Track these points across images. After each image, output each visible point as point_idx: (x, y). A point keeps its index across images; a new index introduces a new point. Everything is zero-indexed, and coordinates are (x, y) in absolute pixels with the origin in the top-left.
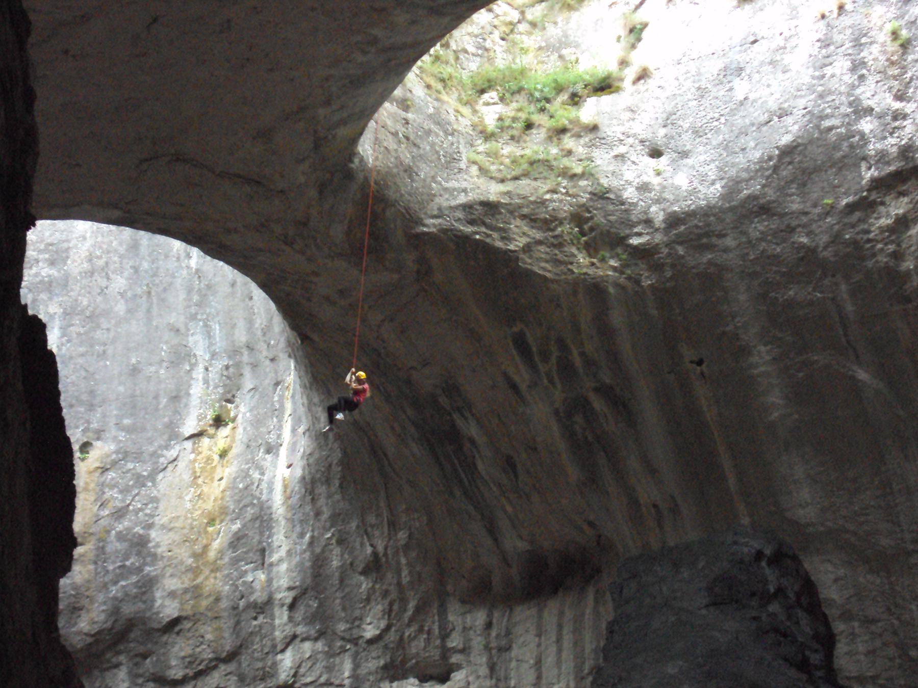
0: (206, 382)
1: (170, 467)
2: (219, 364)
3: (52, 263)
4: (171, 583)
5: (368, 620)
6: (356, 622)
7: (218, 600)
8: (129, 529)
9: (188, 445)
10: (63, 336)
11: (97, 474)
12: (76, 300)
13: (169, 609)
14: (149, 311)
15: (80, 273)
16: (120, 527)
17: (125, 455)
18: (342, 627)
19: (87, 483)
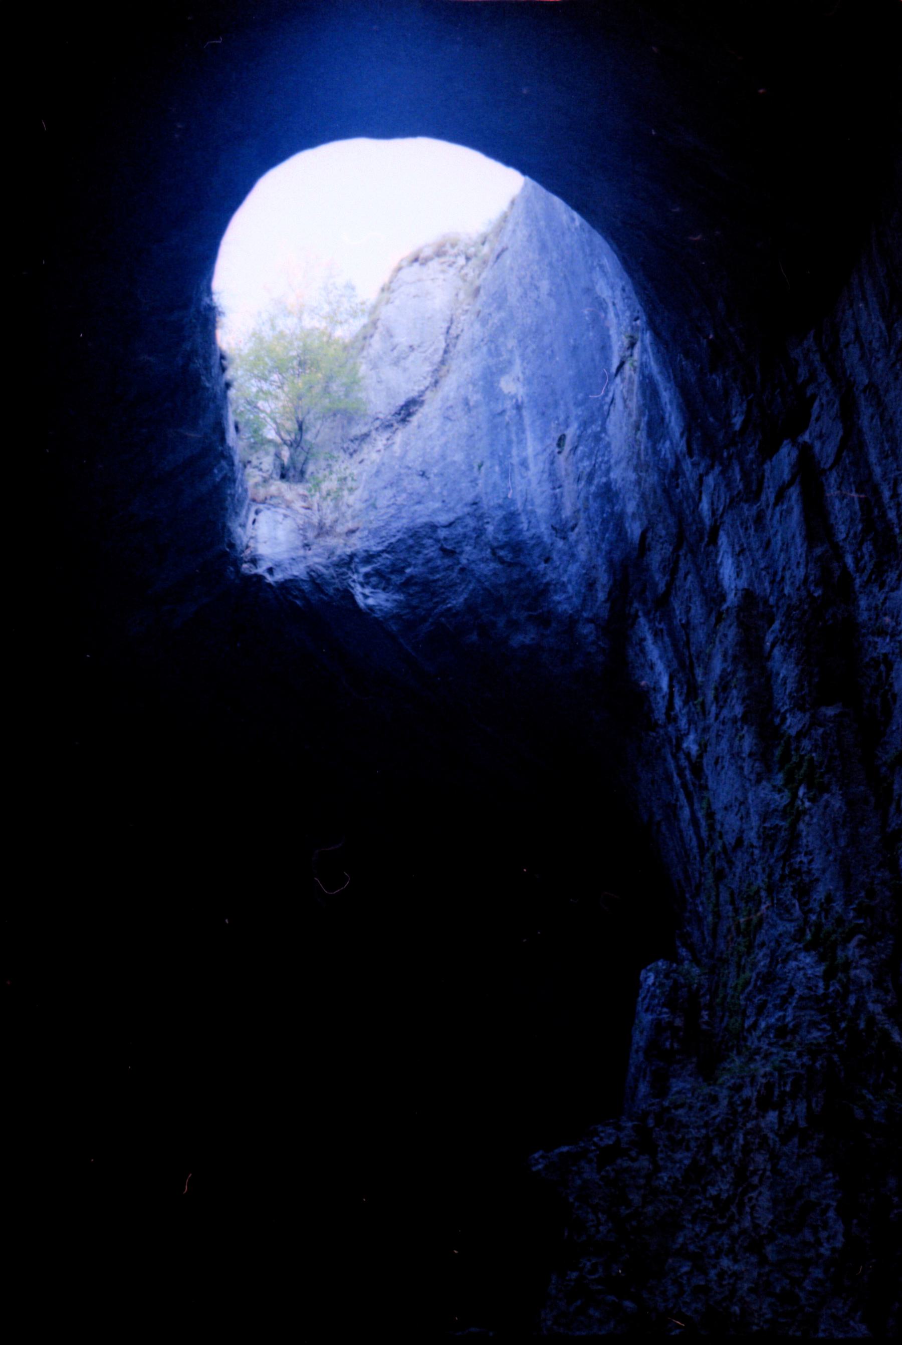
0: (617, 315)
1: (612, 408)
2: (618, 293)
3: (499, 308)
4: (631, 508)
5: (734, 412)
6: (726, 421)
7: (655, 492)
8: (598, 486)
9: (618, 380)
10: (523, 360)
11: (572, 456)
12: (523, 325)
13: (635, 529)
14: (569, 292)
15: (518, 300)
16: (593, 489)
17: (584, 425)
18: (721, 436)
19: (566, 470)
